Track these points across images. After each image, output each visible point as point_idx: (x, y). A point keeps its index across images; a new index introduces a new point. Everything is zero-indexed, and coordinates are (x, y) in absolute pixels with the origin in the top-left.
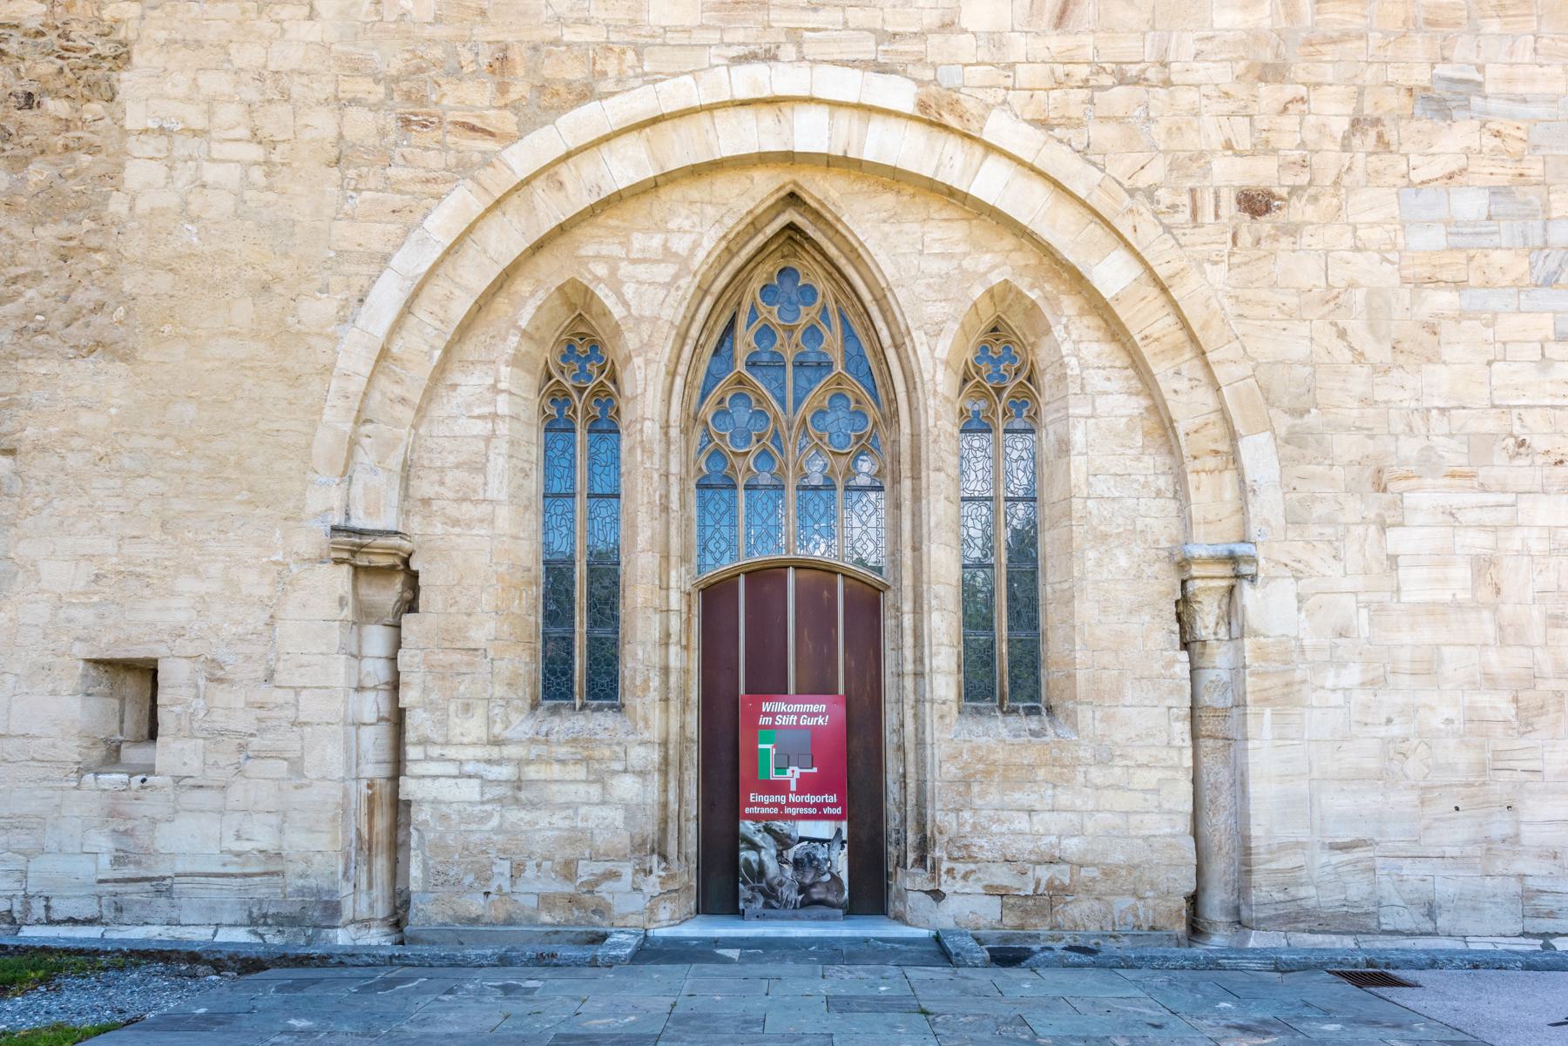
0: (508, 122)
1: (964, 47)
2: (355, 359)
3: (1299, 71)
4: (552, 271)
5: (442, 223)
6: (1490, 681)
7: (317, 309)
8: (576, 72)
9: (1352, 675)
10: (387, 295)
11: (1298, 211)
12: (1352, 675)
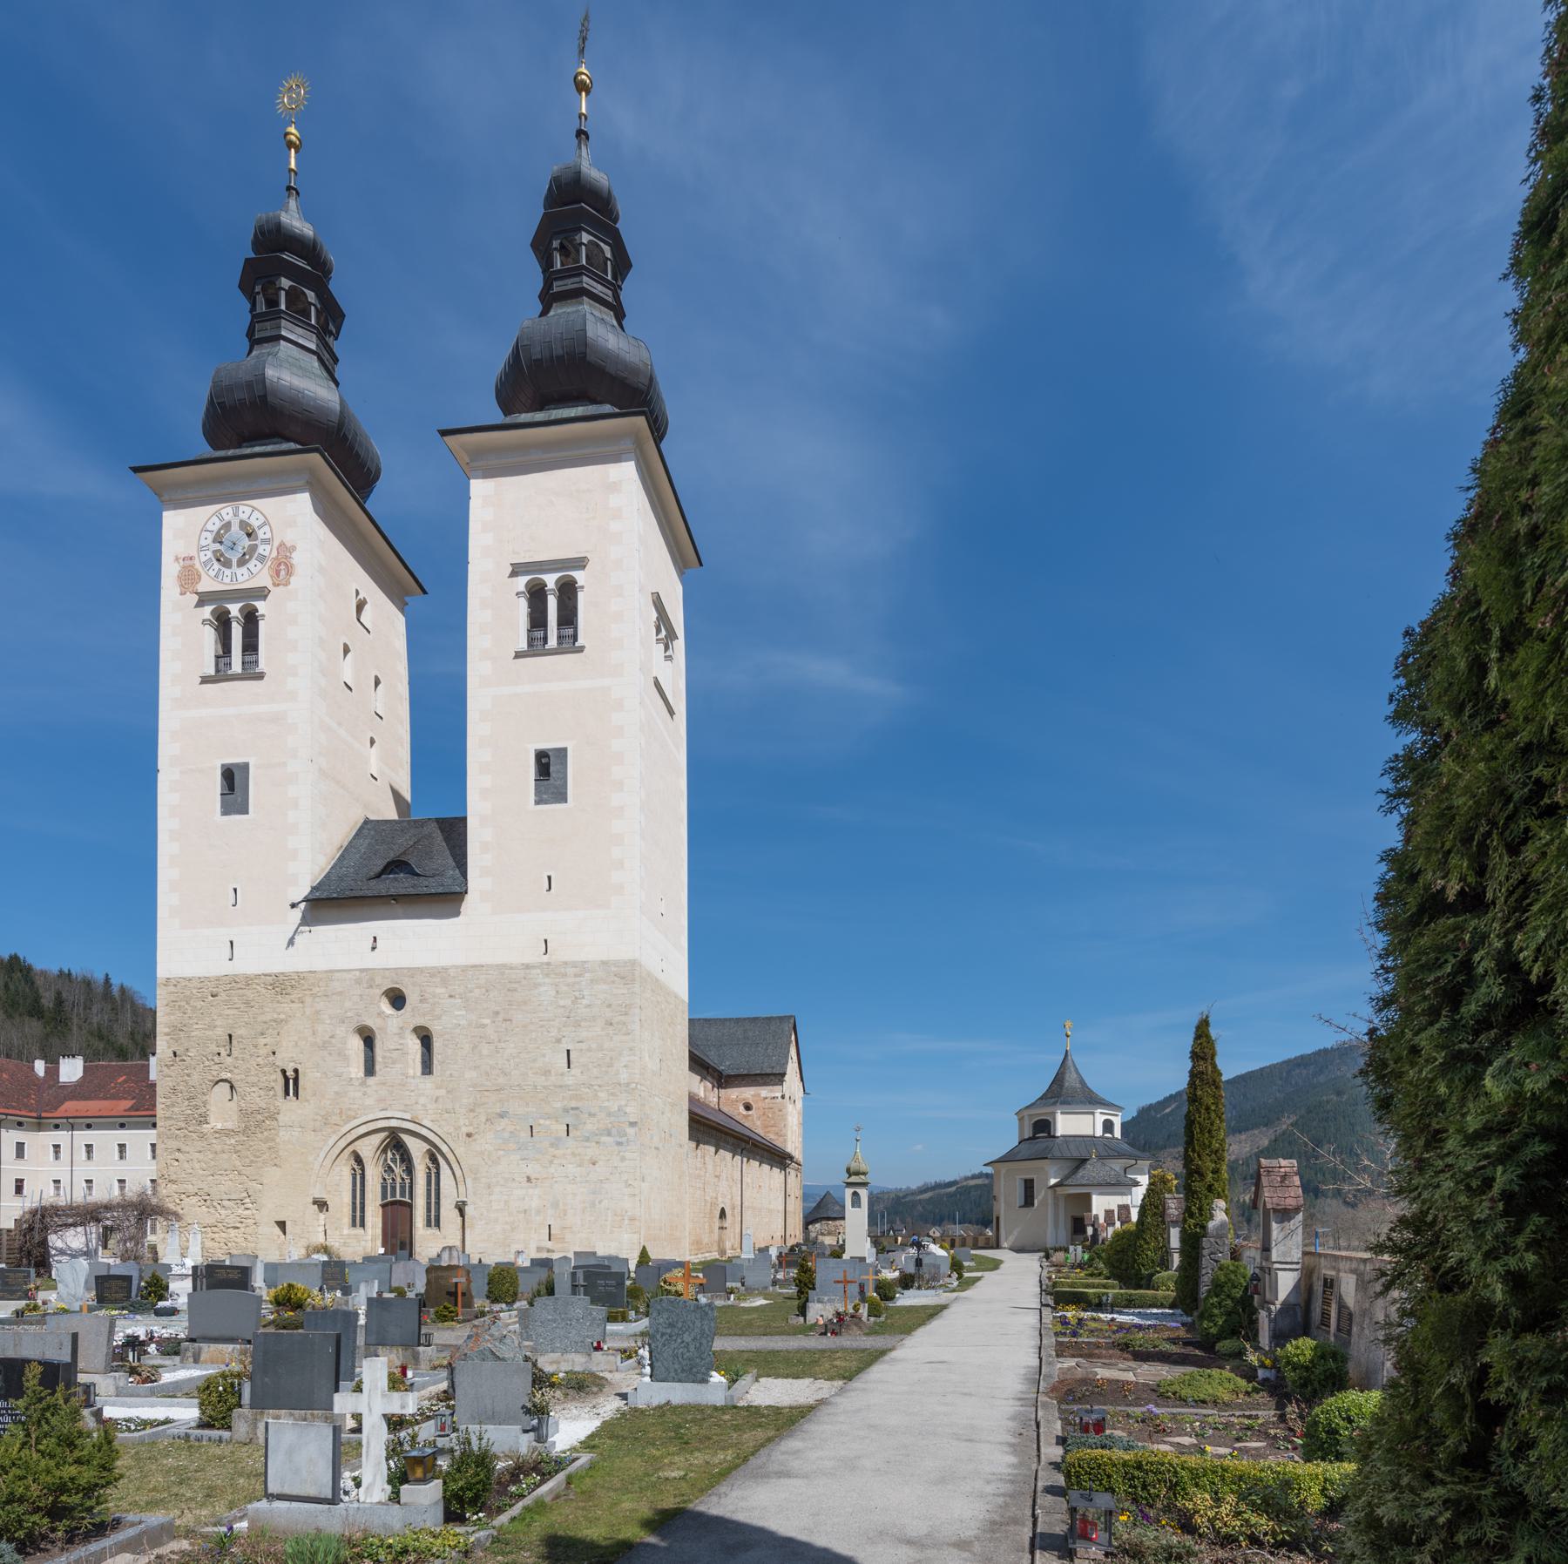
0: (342, 1123)
1: (419, 1107)
2: (317, 1166)
3: (477, 1110)
4: (351, 1148)
5: (331, 1142)
6: (507, 1223)
7: (311, 1158)
8: (353, 1114)
9: (483, 1222)
10: (322, 1155)
11: (476, 1136)
12: (483, 1222)
